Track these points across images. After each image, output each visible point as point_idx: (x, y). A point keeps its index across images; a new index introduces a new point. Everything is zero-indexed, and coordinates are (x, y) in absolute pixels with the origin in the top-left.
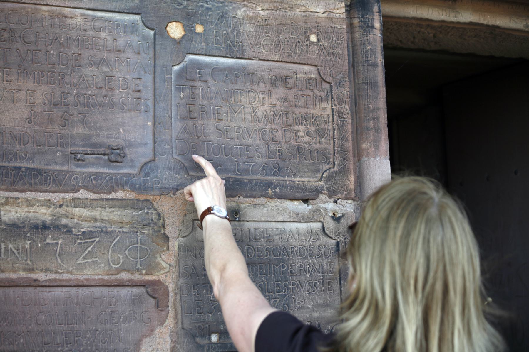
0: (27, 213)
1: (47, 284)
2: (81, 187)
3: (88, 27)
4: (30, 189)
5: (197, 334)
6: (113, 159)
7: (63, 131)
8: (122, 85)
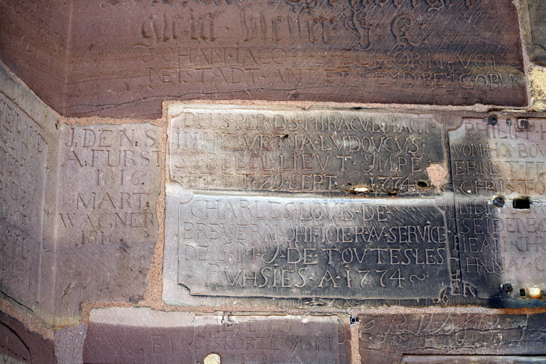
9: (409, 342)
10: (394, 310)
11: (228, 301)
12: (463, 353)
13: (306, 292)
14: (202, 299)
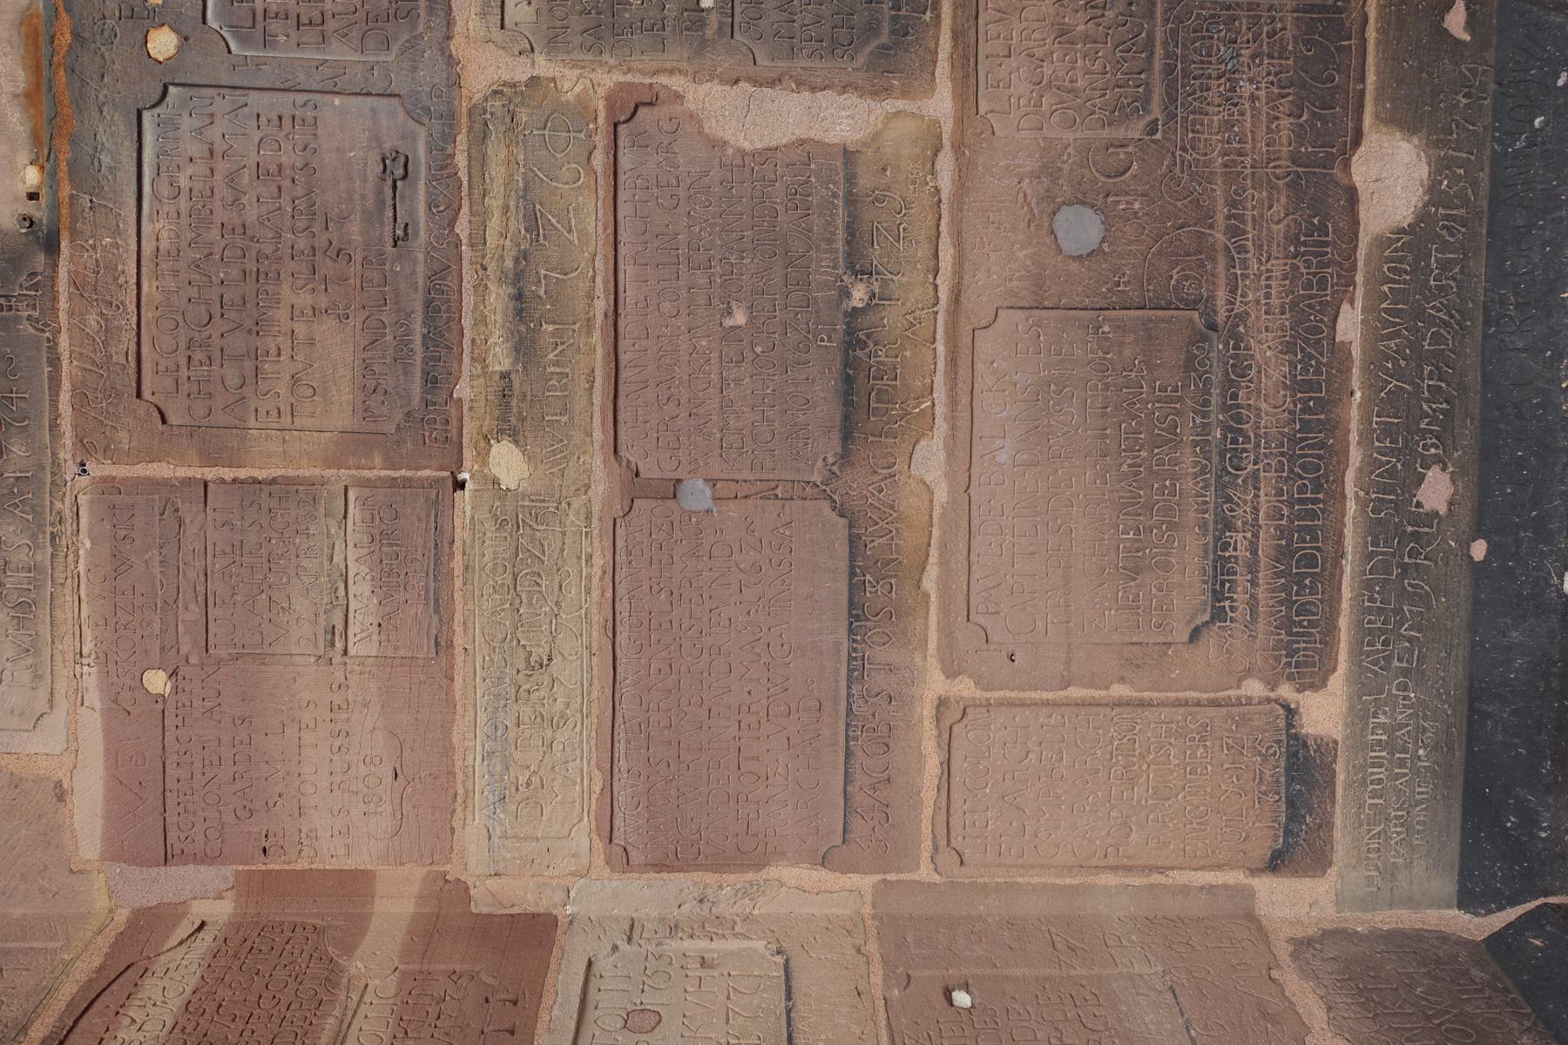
0: (498, 326)
1: (612, 297)
2: (452, 230)
3: (173, 209)
4: (457, 319)
5: (700, 33)
6: (401, 171)
7: (358, 258)
8: (272, 151)
9: (119, 387)
10: (65, 408)
11: (58, 658)
12: (134, 305)
13: (41, 540)
14: (57, 696)
